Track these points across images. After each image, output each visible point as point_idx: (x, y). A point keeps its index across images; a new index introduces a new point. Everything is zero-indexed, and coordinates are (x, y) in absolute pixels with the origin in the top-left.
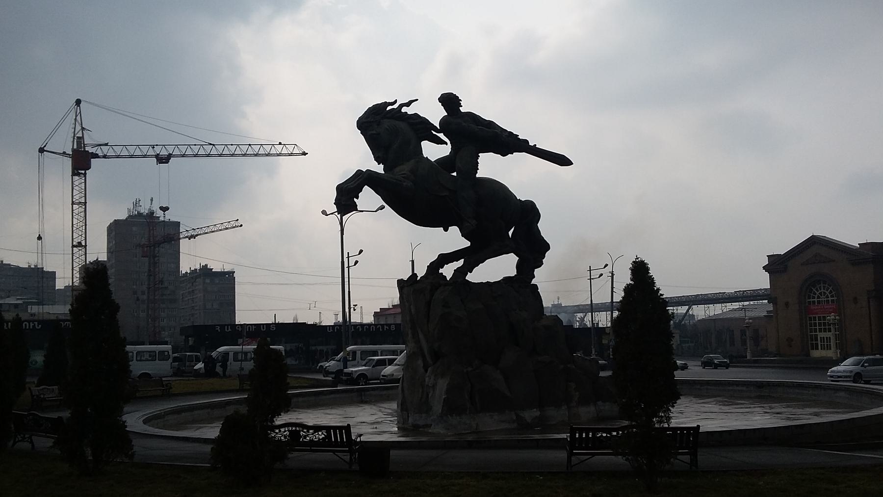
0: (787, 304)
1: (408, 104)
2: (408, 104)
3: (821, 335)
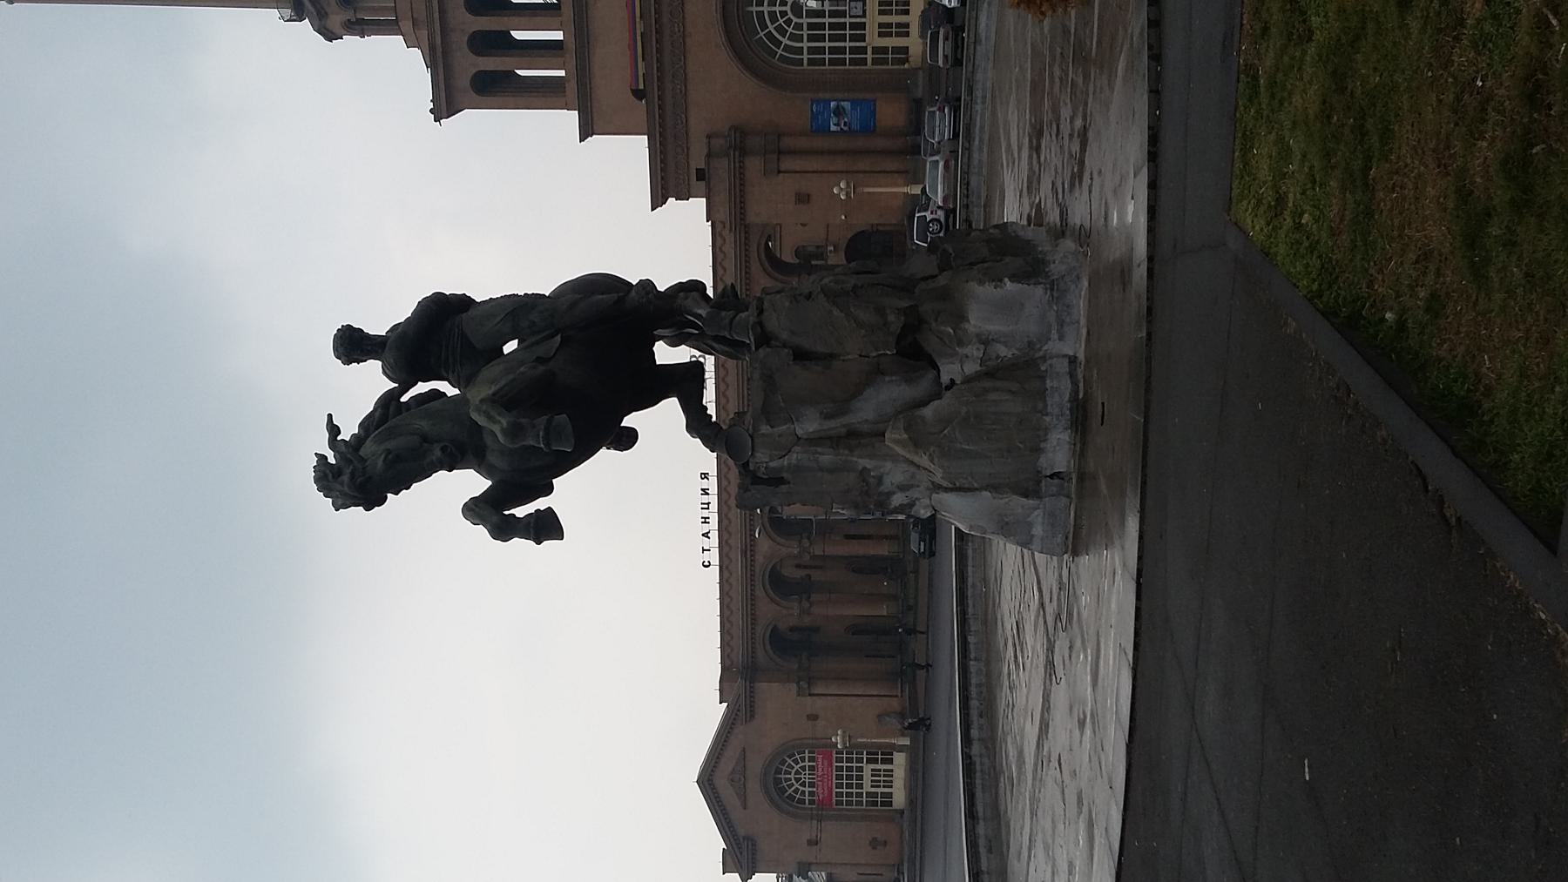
0: (813, 843)
1: (334, 430)
2: (334, 430)
3: (867, 788)
